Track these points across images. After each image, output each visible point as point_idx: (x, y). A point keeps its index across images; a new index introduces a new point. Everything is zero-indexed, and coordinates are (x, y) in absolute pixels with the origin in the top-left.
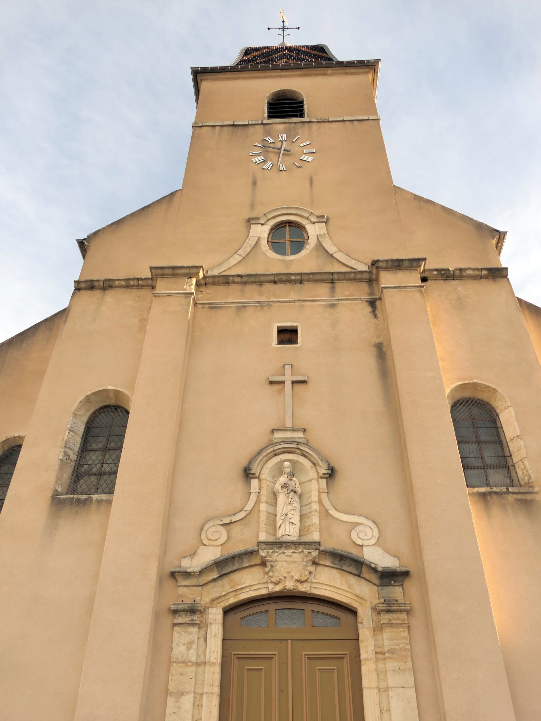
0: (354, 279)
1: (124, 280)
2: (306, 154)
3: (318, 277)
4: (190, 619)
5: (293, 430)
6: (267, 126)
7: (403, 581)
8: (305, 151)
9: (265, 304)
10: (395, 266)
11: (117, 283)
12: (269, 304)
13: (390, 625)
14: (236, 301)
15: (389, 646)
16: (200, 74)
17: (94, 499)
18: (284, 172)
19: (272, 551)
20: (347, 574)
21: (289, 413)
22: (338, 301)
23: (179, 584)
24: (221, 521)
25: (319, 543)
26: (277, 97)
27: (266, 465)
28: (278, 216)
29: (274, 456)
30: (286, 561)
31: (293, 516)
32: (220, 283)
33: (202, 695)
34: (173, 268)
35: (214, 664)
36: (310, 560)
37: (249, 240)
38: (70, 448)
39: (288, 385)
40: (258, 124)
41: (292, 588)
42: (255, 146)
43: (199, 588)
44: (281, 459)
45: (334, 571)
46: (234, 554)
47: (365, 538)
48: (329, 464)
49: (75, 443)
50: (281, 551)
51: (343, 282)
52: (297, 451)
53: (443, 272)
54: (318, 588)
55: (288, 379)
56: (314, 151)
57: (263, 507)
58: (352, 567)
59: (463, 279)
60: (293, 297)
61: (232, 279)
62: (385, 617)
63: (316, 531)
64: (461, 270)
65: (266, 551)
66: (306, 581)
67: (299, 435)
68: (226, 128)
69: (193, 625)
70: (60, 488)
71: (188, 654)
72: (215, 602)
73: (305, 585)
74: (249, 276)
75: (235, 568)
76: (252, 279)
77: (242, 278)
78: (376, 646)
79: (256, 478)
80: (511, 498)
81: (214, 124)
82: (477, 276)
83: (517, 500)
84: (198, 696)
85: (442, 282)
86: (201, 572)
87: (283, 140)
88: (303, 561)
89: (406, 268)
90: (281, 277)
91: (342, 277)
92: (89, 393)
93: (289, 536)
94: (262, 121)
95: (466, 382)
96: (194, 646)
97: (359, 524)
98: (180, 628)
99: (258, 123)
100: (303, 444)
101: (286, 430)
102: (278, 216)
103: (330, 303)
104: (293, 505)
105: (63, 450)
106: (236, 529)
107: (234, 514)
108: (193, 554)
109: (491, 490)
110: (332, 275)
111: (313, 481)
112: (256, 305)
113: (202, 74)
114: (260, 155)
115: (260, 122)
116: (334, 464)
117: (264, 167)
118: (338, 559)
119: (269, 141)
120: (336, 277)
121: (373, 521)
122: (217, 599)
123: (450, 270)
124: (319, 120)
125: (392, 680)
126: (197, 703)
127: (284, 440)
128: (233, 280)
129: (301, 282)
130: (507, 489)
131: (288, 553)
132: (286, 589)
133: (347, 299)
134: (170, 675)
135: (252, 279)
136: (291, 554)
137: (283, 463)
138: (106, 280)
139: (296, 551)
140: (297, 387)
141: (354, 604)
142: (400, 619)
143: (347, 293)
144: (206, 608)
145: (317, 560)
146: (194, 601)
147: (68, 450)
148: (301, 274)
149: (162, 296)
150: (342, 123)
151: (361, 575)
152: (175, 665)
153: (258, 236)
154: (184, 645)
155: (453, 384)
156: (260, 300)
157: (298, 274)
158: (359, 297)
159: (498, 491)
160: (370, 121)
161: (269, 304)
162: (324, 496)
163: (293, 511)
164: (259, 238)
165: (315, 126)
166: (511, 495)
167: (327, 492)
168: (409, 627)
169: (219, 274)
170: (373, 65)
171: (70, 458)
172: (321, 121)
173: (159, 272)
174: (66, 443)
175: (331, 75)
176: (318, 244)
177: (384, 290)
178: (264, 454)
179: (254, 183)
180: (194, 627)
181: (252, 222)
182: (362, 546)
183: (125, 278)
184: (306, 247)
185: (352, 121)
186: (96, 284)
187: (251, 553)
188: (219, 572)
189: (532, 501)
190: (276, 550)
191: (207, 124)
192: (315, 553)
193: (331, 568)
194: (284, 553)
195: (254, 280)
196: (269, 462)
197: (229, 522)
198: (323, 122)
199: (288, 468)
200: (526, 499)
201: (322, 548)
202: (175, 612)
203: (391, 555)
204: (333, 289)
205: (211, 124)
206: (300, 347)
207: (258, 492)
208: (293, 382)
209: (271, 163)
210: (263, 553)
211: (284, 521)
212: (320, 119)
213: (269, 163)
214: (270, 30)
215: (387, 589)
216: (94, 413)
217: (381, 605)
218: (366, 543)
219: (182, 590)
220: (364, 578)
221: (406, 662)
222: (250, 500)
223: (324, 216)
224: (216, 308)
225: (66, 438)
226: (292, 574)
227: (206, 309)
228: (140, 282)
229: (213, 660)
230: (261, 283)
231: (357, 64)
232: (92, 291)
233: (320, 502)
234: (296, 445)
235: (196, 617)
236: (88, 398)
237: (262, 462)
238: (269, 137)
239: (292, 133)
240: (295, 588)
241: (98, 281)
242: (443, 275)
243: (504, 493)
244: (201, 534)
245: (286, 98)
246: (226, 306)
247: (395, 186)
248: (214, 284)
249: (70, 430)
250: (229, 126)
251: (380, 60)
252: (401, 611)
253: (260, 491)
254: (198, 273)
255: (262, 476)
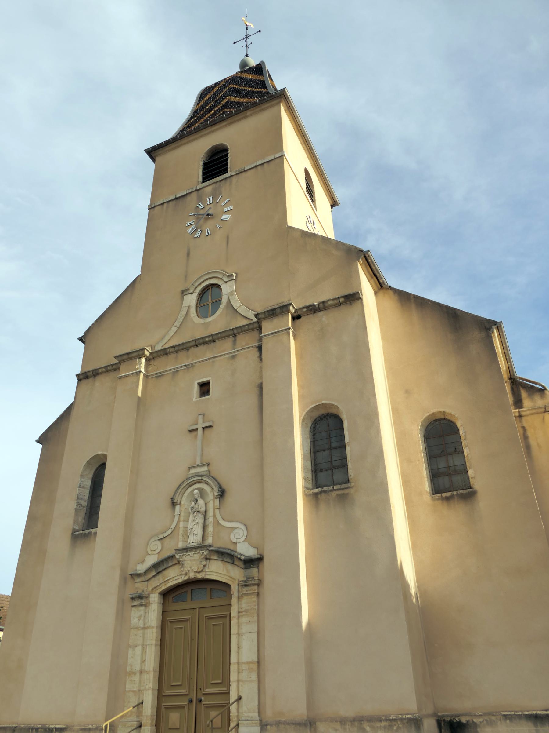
0: (249, 330)
1: (104, 367)
2: (226, 213)
3: (224, 335)
4: (140, 602)
5: (201, 466)
7: (258, 564)
8: (226, 209)
9: (190, 366)
10: (271, 315)
11: (100, 370)
12: (192, 365)
13: (246, 594)
14: (171, 368)
15: (245, 607)
16: (152, 153)
17: (93, 532)
18: (209, 236)
19: (182, 554)
20: (227, 563)
21: (199, 453)
22: (238, 352)
23: (135, 581)
24: (158, 537)
25: (210, 546)
26: (212, 153)
27: (184, 495)
28: (203, 282)
29: (189, 487)
30: (190, 560)
31: (195, 529)
32: (162, 355)
33: (146, 645)
34: (128, 354)
35: (153, 627)
36: (204, 558)
37: (183, 311)
38: (81, 499)
39: (200, 431)
40: (193, 192)
41: (193, 577)
42: (190, 215)
43: (146, 582)
44: (193, 488)
45: (220, 562)
46: (162, 559)
47: (239, 537)
48: (220, 487)
49: (85, 494)
50: (187, 554)
51: (242, 334)
52: (202, 481)
53: (310, 308)
54: (209, 575)
55: (200, 427)
56: (232, 207)
57: (181, 524)
58: (229, 558)
59: (327, 309)
60: (209, 355)
61: (168, 350)
62: (244, 590)
63: (211, 537)
64: (323, 302)
65: (179, 555)
66: (202, 571)
67: (205, 468)
68: (171, 203)
69: (142, 605)
70: (78, 527)
71: (139, 623)
72: (154, 590)
73: (201, 574)
74: (179, 345)
75: (164, 568)
76: (181, 348)
77: (174, 348)
78: (238, 609)
79: (178, 504)
80: (334, 494)
81: (163, 202)
82: (337, 304)
83: (338, 495)
84: (144, 646)
85: (311, 316)
86: (146, 572)
87: (210, 203)
88: (200, 559)
89: (279, 314)
90: (199, 341)
91: (240, 330)
92: (88, 459)
93: (193, 543)
94: (196, 187)
95: (317, 404)
96: (142, 618)
97: (236, 528)
98: (135, 608)
99: (193, 190)
100: (205, 476)
101: (196, 467)
102: (203, 282)
103: (232, 355)
104: (196, 521)
105: (76, 502)
106: (166, 541)
107: (165, 532)
108: (143, 562)
109: (322, 490)
110: (233, 331)
111: (211, 501)
112: (185, 368)
113: (154, 152)
114: (193, 224)
115: (194, 189)
116: (224, 486)
117: (195, 236)
118: (221, 554)
119: (200, 207)
120: (235, 331)
121: (245, 525)
122: (155, 588)
123: (315, 305)
124: (237, 172)
125: (245, 628)
126: (145, 651)
127: (194, 475)
128: (169, 351)
129: (214, 341)
130: (333, 488)
131: (191, 554)
132: (190, 578)
133: (243, 349)
134: (130, 636)
135: (181, 348)
136: (193, 555)
137: (193, 492)
138: (93, 370)
139: (196, 553)
140: (207, 431)
141: (230, 583)
142: (253, 590)
143: (244, 343)
144: (149, 594)
145: (208, 557)
146: (143, 591)
147: (79, 501)
148: (212, 336)
149: (123, 378)
150: (255, 169)
151: (234, 563)
152: (132, 630)
153: (188, 305)
154: (137, 618)
155: (307, 408)
156: (187, 364)
157: (210, 336)
158: (251, 345)
159: (326, 490)
160: (276, 159)
161: (192, 365)
162: (217, 511)
163: (195, 526)
164: (189, 307)
165: (234, 179)
166: (334, 492)
167: (219, 508)
168: (258, 594)
169: (162, 346)
170: (281, 94)
171: (82, 505)
172: (239, 172)
173: (120, 358)
174: (78, 497)
175: (251, 115)
176: (228, 301)
177: (263, 338)
178: (182, 487)
179: (188, 254)
180: (142, 607)
181: (184, 294)
182: (236, 543)
183: (104, 366)
184: (220, 306)
185: (263, 164)
186: (88, 374)
187: (172, 557)
188: (156, 571)
189: (348, 494)
190: (185, 554)
191: (158, 204)
192: (206, 553)
193: (218, 561)
194: (189, 555)
195: (183, 348)
196: (186, 492)
197: (162, 537)
198: (241, 172)
199: (196, 494)
200: (344, 493)
201: (211, 548)
202: (133, 599)
203: (254, 547)
204: (235, 341)
205: (161, 203)
206: (210, 397)
207: (179, 515)
208: (203, 428)
209: (200, 230)
210: (177, 557)
211: (190, 533)
212: (238, 171)
213: (199, 230)
214: (236, 43)
215: (249, 571)
216: (96, 470)
217: (241, 582)
218: (239, 541)
219: (138, 585)
220: (236, 565)
221: (253, 617)
222: (175, 521)
223: (232, 275)
224: (160, 376)
225: (77, 494)
226: (193, 568)
227: (154, 379)
228: (114, 366)
229: (153, 625)
230: (188, 349)
231: (267, 99)
232: (88, 380)
233: (214, 516)
234: (201, 477)
235: (143, 601)
236: (89, 463)
237: (181, 493)
238: (200, 204)
239: (217, 192)
240: (195, 576)
241: (89, 372)
242: (311, 310)
243: (331, 491)
244: (147, 548)
245: (219, 150)
246: (166, 373)
247: (289, 226)
248: (158, 356)
249: (79, 487)
250: (173, 200)
251: (285, 88)
252: (253, 585)
253: (180, 513)
254: (144, 354)
255: (182, 503)
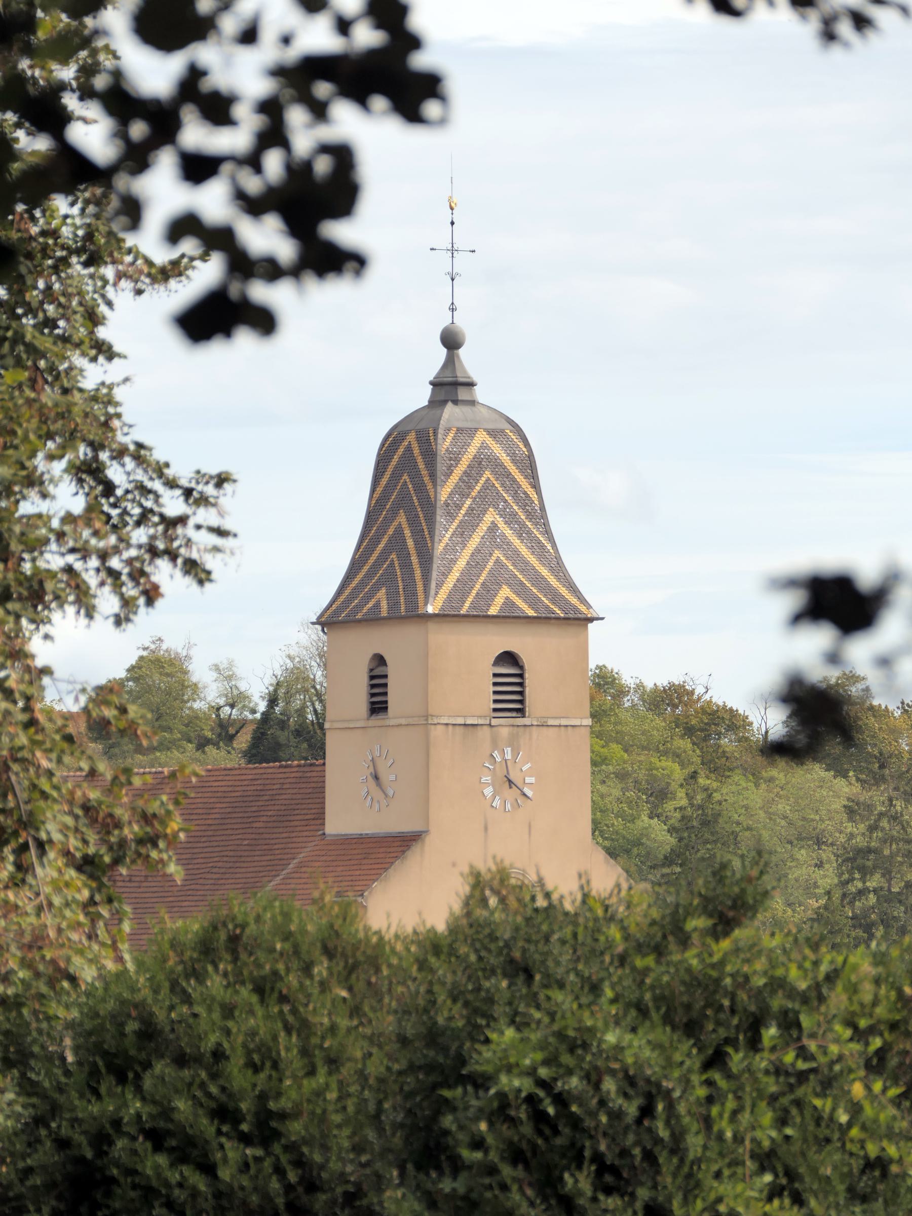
6: (494, 729)
8: (528, 780)
68: (457, 727)
150: (557, 728)
179: (486, 829)
